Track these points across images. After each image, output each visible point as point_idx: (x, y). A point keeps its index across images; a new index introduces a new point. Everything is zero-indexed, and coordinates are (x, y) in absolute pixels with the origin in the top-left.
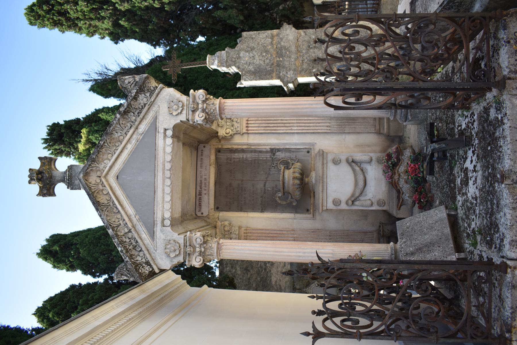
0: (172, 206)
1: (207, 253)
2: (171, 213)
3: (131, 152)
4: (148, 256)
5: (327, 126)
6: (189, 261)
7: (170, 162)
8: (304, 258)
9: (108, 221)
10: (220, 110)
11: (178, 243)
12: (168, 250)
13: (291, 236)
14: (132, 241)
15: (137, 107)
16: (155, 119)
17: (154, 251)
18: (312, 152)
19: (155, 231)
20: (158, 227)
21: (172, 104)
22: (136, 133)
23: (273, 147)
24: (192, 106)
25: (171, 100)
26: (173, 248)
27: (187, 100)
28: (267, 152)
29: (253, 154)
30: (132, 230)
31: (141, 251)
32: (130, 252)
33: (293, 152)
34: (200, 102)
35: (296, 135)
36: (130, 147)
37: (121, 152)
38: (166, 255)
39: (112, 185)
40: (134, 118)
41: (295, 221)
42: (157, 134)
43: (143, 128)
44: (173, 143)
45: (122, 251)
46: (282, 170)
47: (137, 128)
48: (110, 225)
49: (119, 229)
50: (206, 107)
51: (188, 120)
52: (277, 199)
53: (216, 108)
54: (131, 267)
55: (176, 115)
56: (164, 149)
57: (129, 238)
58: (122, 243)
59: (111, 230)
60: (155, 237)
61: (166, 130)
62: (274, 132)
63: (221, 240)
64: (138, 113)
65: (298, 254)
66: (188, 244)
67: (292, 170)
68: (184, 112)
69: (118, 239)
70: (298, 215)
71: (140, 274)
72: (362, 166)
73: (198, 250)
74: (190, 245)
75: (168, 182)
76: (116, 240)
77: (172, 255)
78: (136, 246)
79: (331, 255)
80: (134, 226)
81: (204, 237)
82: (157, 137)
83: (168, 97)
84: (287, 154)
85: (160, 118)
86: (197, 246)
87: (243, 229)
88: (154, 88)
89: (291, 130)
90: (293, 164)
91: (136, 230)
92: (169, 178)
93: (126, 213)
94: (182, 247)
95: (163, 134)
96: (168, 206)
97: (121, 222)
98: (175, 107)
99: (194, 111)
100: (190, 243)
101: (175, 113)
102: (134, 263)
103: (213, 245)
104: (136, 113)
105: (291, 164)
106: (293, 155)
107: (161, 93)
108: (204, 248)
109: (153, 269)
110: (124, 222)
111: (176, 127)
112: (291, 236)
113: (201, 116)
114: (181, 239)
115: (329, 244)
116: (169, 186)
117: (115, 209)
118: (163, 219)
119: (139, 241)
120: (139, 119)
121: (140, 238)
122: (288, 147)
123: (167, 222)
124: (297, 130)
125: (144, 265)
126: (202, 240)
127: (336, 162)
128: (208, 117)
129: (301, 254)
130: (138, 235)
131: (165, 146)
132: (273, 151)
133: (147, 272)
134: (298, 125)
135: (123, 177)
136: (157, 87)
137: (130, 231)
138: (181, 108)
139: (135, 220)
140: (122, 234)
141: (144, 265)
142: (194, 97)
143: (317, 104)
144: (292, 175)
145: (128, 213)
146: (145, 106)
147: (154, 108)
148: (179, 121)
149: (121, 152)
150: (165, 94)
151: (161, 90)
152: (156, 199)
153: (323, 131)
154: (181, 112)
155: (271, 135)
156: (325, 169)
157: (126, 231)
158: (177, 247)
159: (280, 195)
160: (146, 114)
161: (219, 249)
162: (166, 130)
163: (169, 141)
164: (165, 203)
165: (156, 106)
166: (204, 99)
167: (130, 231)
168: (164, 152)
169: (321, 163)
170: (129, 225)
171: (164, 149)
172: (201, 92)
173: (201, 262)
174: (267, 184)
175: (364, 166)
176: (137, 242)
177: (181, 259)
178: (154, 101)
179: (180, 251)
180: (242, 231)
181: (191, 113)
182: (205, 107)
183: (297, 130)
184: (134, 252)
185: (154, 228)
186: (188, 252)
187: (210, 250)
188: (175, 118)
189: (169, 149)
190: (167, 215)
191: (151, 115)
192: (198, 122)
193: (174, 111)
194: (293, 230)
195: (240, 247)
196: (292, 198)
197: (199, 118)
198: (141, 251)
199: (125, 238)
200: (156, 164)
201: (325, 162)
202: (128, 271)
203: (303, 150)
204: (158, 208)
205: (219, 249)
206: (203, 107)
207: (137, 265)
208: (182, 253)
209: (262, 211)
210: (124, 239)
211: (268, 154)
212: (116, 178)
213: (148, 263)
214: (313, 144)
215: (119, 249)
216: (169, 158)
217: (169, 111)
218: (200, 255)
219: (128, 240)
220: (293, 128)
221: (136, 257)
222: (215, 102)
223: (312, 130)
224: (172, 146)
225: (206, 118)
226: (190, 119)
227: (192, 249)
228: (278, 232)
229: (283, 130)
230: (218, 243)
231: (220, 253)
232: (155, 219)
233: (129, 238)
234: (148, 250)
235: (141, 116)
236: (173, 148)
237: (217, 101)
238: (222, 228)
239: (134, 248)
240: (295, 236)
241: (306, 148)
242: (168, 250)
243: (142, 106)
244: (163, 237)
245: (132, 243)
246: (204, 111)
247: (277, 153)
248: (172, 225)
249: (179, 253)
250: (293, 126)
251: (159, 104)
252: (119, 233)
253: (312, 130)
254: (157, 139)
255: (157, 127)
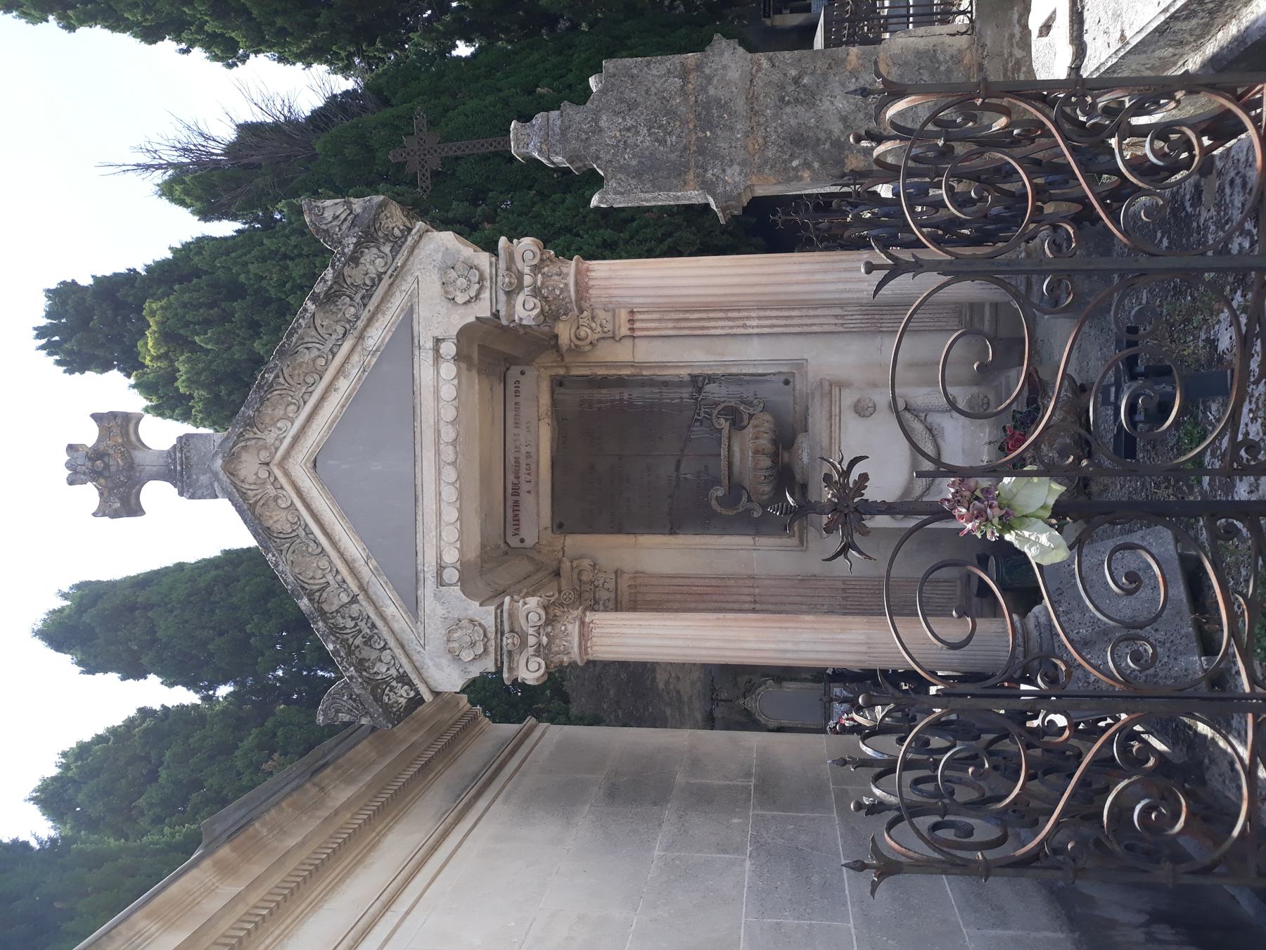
0: (461, 532)
1: (555, 649)
2: (461, 550)
3: (347, 399)
4: (404, 660)
5: (836, 316)
6: (511, 669)
7: (452, 423)
8: (795, 656)
9: (296, 578)
10: (577, 291)
11: (480, 625)
12: (455, 645)
13: (746, 591)
14: (362, 624)
15: (359, 282)
16: (409, 313)
17: (419, 649)
18: (797, 382)
19: (421, 598)
20: (428, 590)
21: (453, 274)
22: (359, 348)
23: (696, 372)
24: (507, 280)
25: (450, 263)
26: (468, 639)
27: (491, 264)
28: (681, 384)
29: (647, 390)
30: (360, 597)
31: (384, 648)
32: (357, 653)
33: (748, 382)
34: (527, 270)
35: (756, 340)
36: (344, 385)
37: (323, 398)
38: (449, 656)
39: (300, 483)
40: (352, 310)
41: (755, 554)
42: (417, 353)
43: (377, 335)
44: (458, 375)
45: (336, 652)
46: (725, 432)
47: (361, 337)
48: (303, 588)
49: (325, 595)
50: (542, 283)
51: (496, 315)
52: (714, 502)
53: (566, 285)
54: (362, 692)
55: (465, 303)
56: (437, 391)
57: (353, 619)
58: (335, 630)
59: (305, 600)
60: (421, 613)
61: (438, 341)
62: (700, 332)
63: (588, 613)
64: (363, 298)
65: (782, 646)
66: (507, 628)
67: (749, 432)
68: (486, 295)
69: (324, 621)
70: (763, 541)
71: (387, 708)
72: (929, 419)
73: (532, 640)
74: (512, 631)
75: (450, 474)
76: (320, 624)
77: (467, 656)
78: (372, 637)
79: (864, 649)
80: (362, 588)
81: (545, 608)
82: (416, 359)
83: (439, 256)
84: (733, 389)
85: (423, 312)
86: (531, 631)
87: (625, 576)
88: (401, 231)
89: (744, 326)
90: (751, 416)
91: (369, 598)
92: (454, 463)
93: (342, 555)
94: (492, 635)
95: (431, 353)
96: (451, 534)
97: (330, 578)
98: (462, 282)
99: (510, 294)
100: (512, 624)
101: (461, 298)
102: (368, 681)
103: (570, 627)
104: (358, 298)
105: (746, 417)
106: (747, 392)
107: (422, 244)
108: (548, 635)
109: (418, 693)
110: (339, 577)
111: (465, 334)
112: (746, 591)
113: (530, 305)
114: (486, 614)
115: (858, 619)
116: (453, 484)
117: (312, 544)
118: (441, 568)
119: (379, 623)
120: (365, 315)
121: (384, 619)
122: (734, 370)
123: (452, 575)
124: (758, 327)
125: (394, 683)
126: (544, 617)
127: (863, 410)
128: (547, 308)
129: (789, 646)
130: (376, 608)
131: (440, 384)
132: (698, 382)
133: (403, 701)
134: (762, 313)
135: (330, 462)
136: (410, 230)
137: (354, 600)
138: (477, 286)
139: (365, 572)
140: (334, 608)
141: (394, 683)
142: (511, 258)
143: (826, 272)
144: (750, 445)
145: (347, 555)
146: (380, 280)
147: (406, 285)
148: (472, 319)
149: (323, 398)
150: (432, 246)
151: (421, 237)
152: (419, 518)
153: (826, 328)
154: (477, 296)
155: (692, 340)
156: (835, 428)
157: (345, 598)
158: (478, 636)
159: (720, 493)
160: (383, 300)
161: (584, 636)
162: (438, 341)
163: (449, 370)
164: (444, 528)
165: (410, 279)
166: (536, 261)
167: (354, 600)
168: (437, 398)
169: (825, 413)
170: (352, 585)
171: (437, 391)
172: (527, 245)
173: (542, 670)
174: (683, 465)
175: (935, 419)
176: (374, 626)
177: (489, 665)
178: (403, 266)
179: (485, 645)
180: (624, 583)
181: (502, 297)
182: (539, 283)
183: (758, 327)
184: (366, 653)
185: (417, 589)
186: (510, 647)
187: (561, 639)
188: (462, 310)
189: (448, 392)
190: (451, 556)
191: (397, 303)
192: (525, 322)
193: (458, 293)
194: (751, 577)
195: (637, 631)
196: (749, 500)
197: (525, 311)
198: (384, 648)
199: (343, 617)
200: (418, 430)
201: (836, 410)
202: (354, 701)
203: (773, 378)
204: (427, 538)
205: (584, 636)
206: (535, 282)
207: (377, 686)
208: (492, 649)
209: (672, 532)
210: (341, 621)
211: (684, 390)
212: (310, 465)
213: (404, 679)
214: (800, 365)
215: (330, 647)
216: (449, 413)
217: (446, 292)
218: (537, 653)
219: (350, 624)
220: (748, 323)
221: (374, 665)
222: (564, 270)
223: (798, 326)
224: (456, 382)
225: (542, 310)
226: (502, 313)
227: (517, 641)
228: (714, 582)
229: (723, 327)
230: (582, 623)
231: (586, 648)
232: (420, 568)
233: (353, 619)
234: (403, 647)
235: (371, 307)
236: (459, 389)
237: (571, 267)
238: (575, 576)
239: (368, 641)
240: (757, 591)
241: (780, 373)
242: (455, 645)
243: (372, 280)
244: (440, 611)
245: (360, 631)
246: (536, 292)
247: (708, 388)
248: (463, 582)
249: (485, 650)
250: (748, 318)
251: (418, 273)
252: (325, 607)
253: (798, 326)
254: (416, 366)
255: (415, 334)
